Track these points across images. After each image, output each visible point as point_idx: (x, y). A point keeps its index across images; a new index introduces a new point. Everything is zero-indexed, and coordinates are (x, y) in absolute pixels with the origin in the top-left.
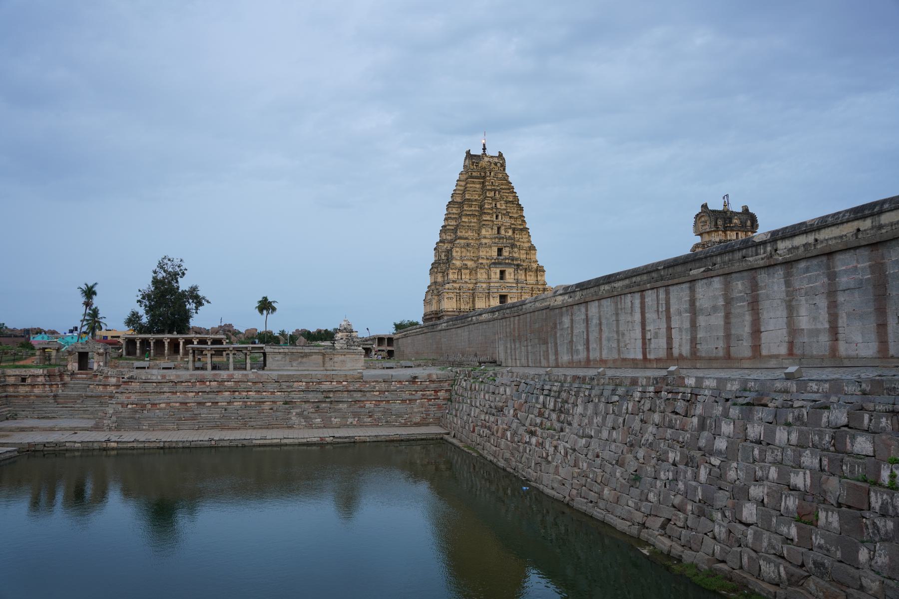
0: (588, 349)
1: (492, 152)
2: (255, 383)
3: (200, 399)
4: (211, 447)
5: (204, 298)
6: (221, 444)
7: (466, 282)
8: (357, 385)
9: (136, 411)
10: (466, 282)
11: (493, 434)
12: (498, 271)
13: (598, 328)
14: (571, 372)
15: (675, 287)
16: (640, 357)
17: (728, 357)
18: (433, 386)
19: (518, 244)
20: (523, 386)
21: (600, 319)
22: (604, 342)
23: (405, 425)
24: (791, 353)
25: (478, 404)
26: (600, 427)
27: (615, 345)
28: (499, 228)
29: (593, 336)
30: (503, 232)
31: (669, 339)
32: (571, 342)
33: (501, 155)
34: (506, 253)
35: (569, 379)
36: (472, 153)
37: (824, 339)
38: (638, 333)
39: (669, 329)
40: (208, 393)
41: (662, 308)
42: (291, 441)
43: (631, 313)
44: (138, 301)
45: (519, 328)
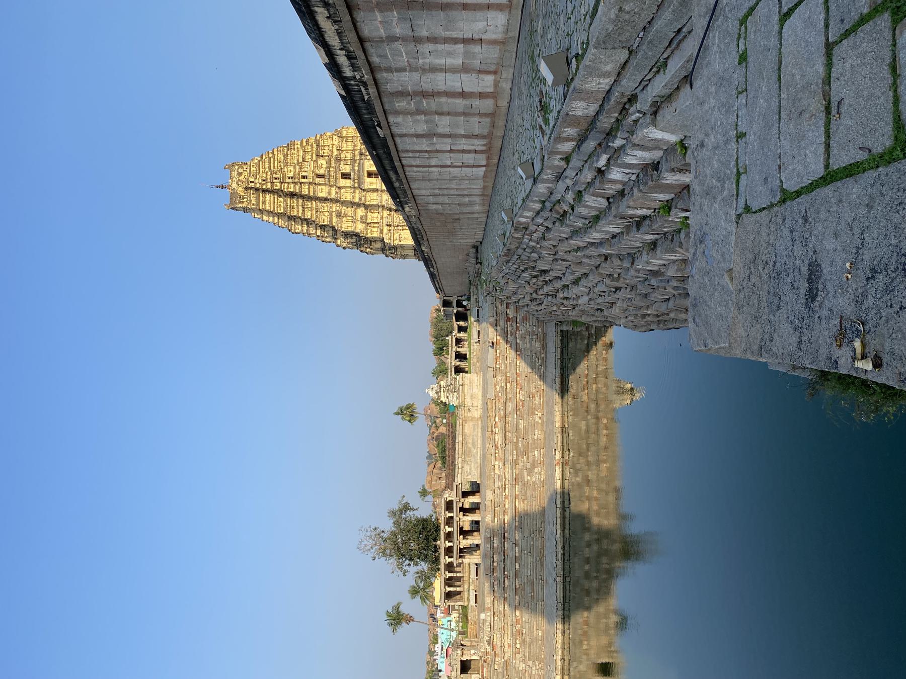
3: (512, 574)
4: (564, 581)
5: (400, 502)
6: (560, 571)
7: (382, 218)
8: (499, 405)
9: (523, 642)
10: (382, 218)
16: (484, 169)
17: (493, 115)
18: (501, 323)
19: (335, 153)
23: (544, 360)
24: (495, 73)
28: (318, 176)
29: (452, 192)
30: (322, 172)
34: (347, 169)
37: (477, 49)
39: (451, 151)
41: (427, 155)
42: (558, 496)
44: (405, 575)
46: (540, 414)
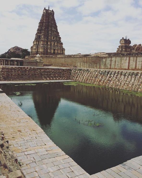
0: (111, 66)
1: (51, 9)
2: (33, 70)
7: (46, 45)
11: (95, 81)
12: (53, 43)
13: (114, 62)
14: (117, 71)
15: (139, 57)
20: (100, 72)
21: (115, 61)
22: (116, 65)
25: (86, 75)
26: (131, 80)
27: (120, 66)
28: (53, 32)
31: (136, 66)
32: (105, 64)
33: (53, 10)
35: (117, 72)
36: (46, 9)
38: (127, 64)
39: (136, 64)
40: (23, 72)
43: (126, 61)
45: (86, 60)
46: (55, 79)
